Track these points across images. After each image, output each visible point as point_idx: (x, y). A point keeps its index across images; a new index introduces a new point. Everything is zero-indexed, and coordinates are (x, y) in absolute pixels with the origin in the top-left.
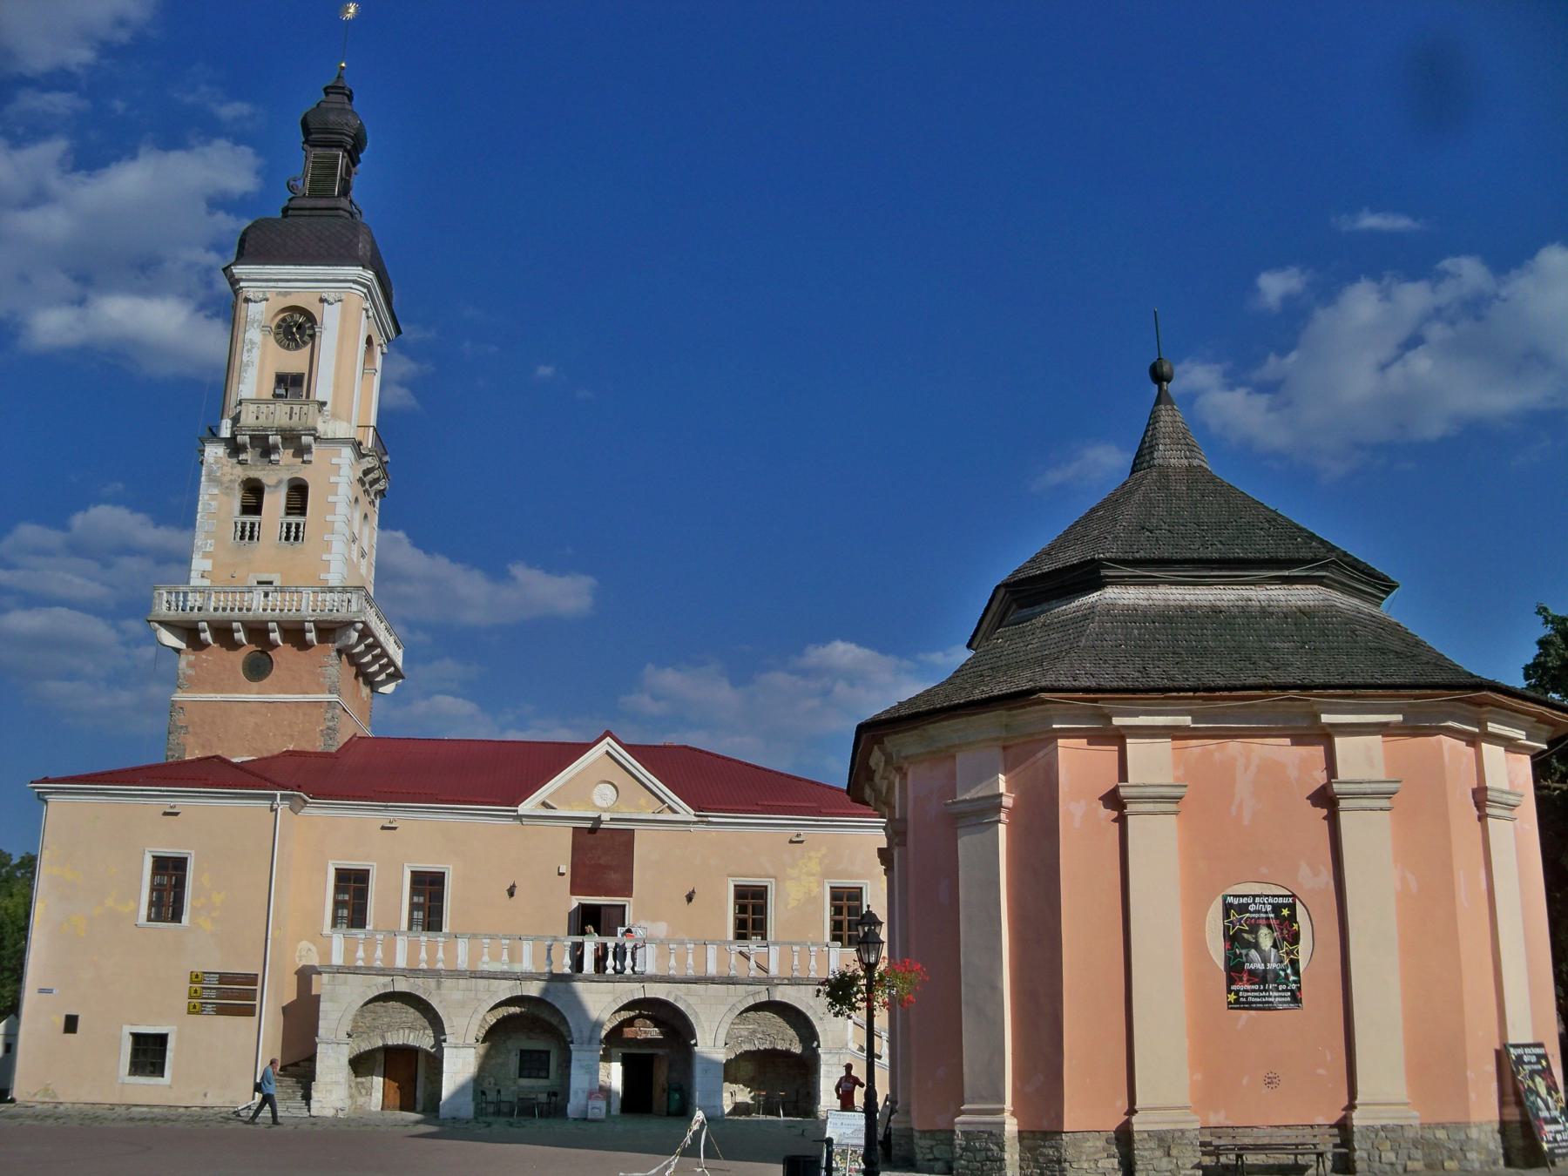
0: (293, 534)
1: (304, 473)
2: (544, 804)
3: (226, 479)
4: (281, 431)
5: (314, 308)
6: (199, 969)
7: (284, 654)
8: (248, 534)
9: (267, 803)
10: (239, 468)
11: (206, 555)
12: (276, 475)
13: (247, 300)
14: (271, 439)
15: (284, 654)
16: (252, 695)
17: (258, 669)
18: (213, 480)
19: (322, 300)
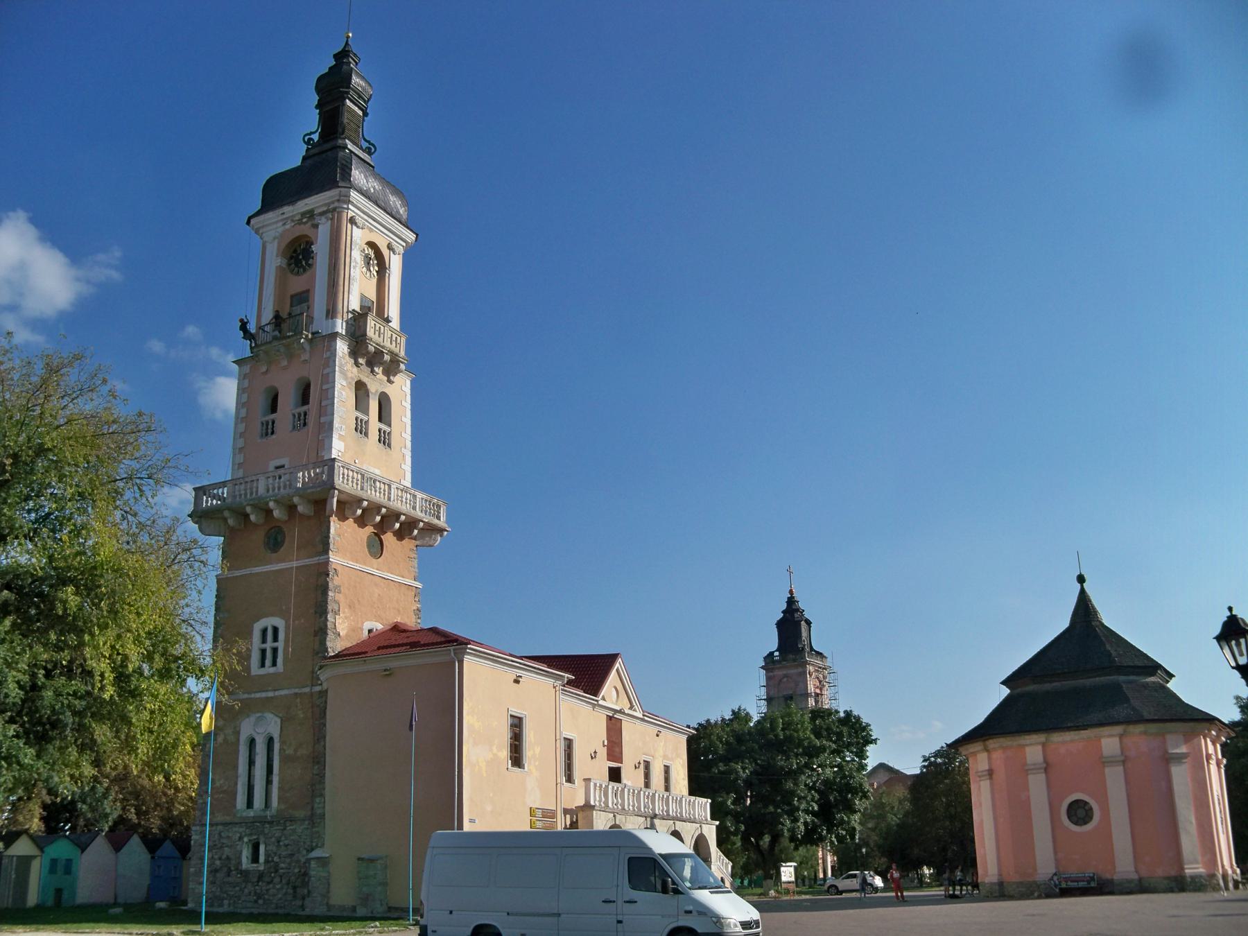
0: (385, 439)
1: (390, 390)
2: (603, 699)
3: (350, 375)
4: (391, 353)
5: (385, 252)
6: (534, 806)
7: (389, 538)
8: (361, 428)
9: (551, 681)
10: (355, 369)
11: (341, 437)
12: (376, 383)
13: (352, 221)
14: (387, 358)
15: (389, 538)
16: (374, 567)
17: (376, 547)
18: (343, 373)
19: (390, 247)
